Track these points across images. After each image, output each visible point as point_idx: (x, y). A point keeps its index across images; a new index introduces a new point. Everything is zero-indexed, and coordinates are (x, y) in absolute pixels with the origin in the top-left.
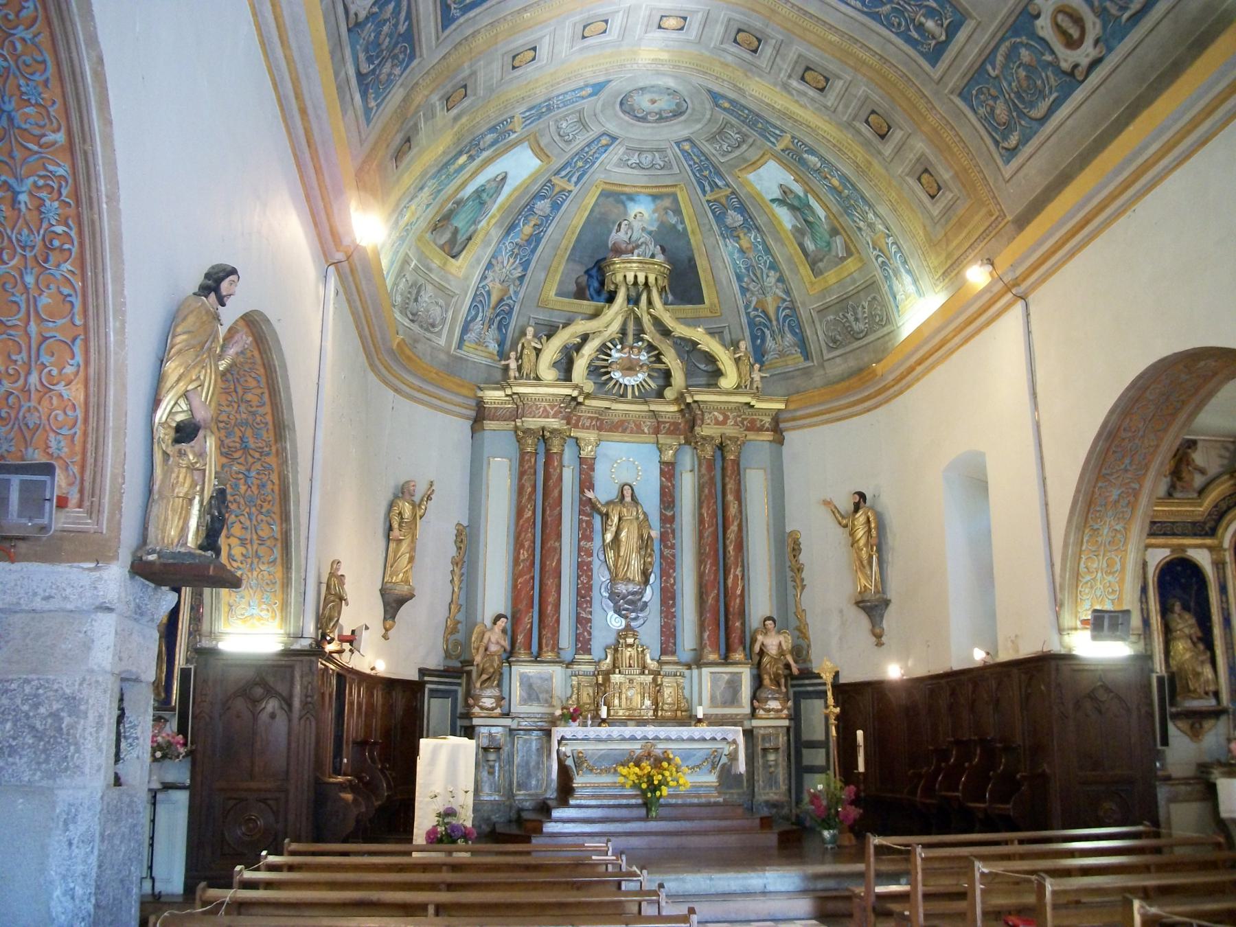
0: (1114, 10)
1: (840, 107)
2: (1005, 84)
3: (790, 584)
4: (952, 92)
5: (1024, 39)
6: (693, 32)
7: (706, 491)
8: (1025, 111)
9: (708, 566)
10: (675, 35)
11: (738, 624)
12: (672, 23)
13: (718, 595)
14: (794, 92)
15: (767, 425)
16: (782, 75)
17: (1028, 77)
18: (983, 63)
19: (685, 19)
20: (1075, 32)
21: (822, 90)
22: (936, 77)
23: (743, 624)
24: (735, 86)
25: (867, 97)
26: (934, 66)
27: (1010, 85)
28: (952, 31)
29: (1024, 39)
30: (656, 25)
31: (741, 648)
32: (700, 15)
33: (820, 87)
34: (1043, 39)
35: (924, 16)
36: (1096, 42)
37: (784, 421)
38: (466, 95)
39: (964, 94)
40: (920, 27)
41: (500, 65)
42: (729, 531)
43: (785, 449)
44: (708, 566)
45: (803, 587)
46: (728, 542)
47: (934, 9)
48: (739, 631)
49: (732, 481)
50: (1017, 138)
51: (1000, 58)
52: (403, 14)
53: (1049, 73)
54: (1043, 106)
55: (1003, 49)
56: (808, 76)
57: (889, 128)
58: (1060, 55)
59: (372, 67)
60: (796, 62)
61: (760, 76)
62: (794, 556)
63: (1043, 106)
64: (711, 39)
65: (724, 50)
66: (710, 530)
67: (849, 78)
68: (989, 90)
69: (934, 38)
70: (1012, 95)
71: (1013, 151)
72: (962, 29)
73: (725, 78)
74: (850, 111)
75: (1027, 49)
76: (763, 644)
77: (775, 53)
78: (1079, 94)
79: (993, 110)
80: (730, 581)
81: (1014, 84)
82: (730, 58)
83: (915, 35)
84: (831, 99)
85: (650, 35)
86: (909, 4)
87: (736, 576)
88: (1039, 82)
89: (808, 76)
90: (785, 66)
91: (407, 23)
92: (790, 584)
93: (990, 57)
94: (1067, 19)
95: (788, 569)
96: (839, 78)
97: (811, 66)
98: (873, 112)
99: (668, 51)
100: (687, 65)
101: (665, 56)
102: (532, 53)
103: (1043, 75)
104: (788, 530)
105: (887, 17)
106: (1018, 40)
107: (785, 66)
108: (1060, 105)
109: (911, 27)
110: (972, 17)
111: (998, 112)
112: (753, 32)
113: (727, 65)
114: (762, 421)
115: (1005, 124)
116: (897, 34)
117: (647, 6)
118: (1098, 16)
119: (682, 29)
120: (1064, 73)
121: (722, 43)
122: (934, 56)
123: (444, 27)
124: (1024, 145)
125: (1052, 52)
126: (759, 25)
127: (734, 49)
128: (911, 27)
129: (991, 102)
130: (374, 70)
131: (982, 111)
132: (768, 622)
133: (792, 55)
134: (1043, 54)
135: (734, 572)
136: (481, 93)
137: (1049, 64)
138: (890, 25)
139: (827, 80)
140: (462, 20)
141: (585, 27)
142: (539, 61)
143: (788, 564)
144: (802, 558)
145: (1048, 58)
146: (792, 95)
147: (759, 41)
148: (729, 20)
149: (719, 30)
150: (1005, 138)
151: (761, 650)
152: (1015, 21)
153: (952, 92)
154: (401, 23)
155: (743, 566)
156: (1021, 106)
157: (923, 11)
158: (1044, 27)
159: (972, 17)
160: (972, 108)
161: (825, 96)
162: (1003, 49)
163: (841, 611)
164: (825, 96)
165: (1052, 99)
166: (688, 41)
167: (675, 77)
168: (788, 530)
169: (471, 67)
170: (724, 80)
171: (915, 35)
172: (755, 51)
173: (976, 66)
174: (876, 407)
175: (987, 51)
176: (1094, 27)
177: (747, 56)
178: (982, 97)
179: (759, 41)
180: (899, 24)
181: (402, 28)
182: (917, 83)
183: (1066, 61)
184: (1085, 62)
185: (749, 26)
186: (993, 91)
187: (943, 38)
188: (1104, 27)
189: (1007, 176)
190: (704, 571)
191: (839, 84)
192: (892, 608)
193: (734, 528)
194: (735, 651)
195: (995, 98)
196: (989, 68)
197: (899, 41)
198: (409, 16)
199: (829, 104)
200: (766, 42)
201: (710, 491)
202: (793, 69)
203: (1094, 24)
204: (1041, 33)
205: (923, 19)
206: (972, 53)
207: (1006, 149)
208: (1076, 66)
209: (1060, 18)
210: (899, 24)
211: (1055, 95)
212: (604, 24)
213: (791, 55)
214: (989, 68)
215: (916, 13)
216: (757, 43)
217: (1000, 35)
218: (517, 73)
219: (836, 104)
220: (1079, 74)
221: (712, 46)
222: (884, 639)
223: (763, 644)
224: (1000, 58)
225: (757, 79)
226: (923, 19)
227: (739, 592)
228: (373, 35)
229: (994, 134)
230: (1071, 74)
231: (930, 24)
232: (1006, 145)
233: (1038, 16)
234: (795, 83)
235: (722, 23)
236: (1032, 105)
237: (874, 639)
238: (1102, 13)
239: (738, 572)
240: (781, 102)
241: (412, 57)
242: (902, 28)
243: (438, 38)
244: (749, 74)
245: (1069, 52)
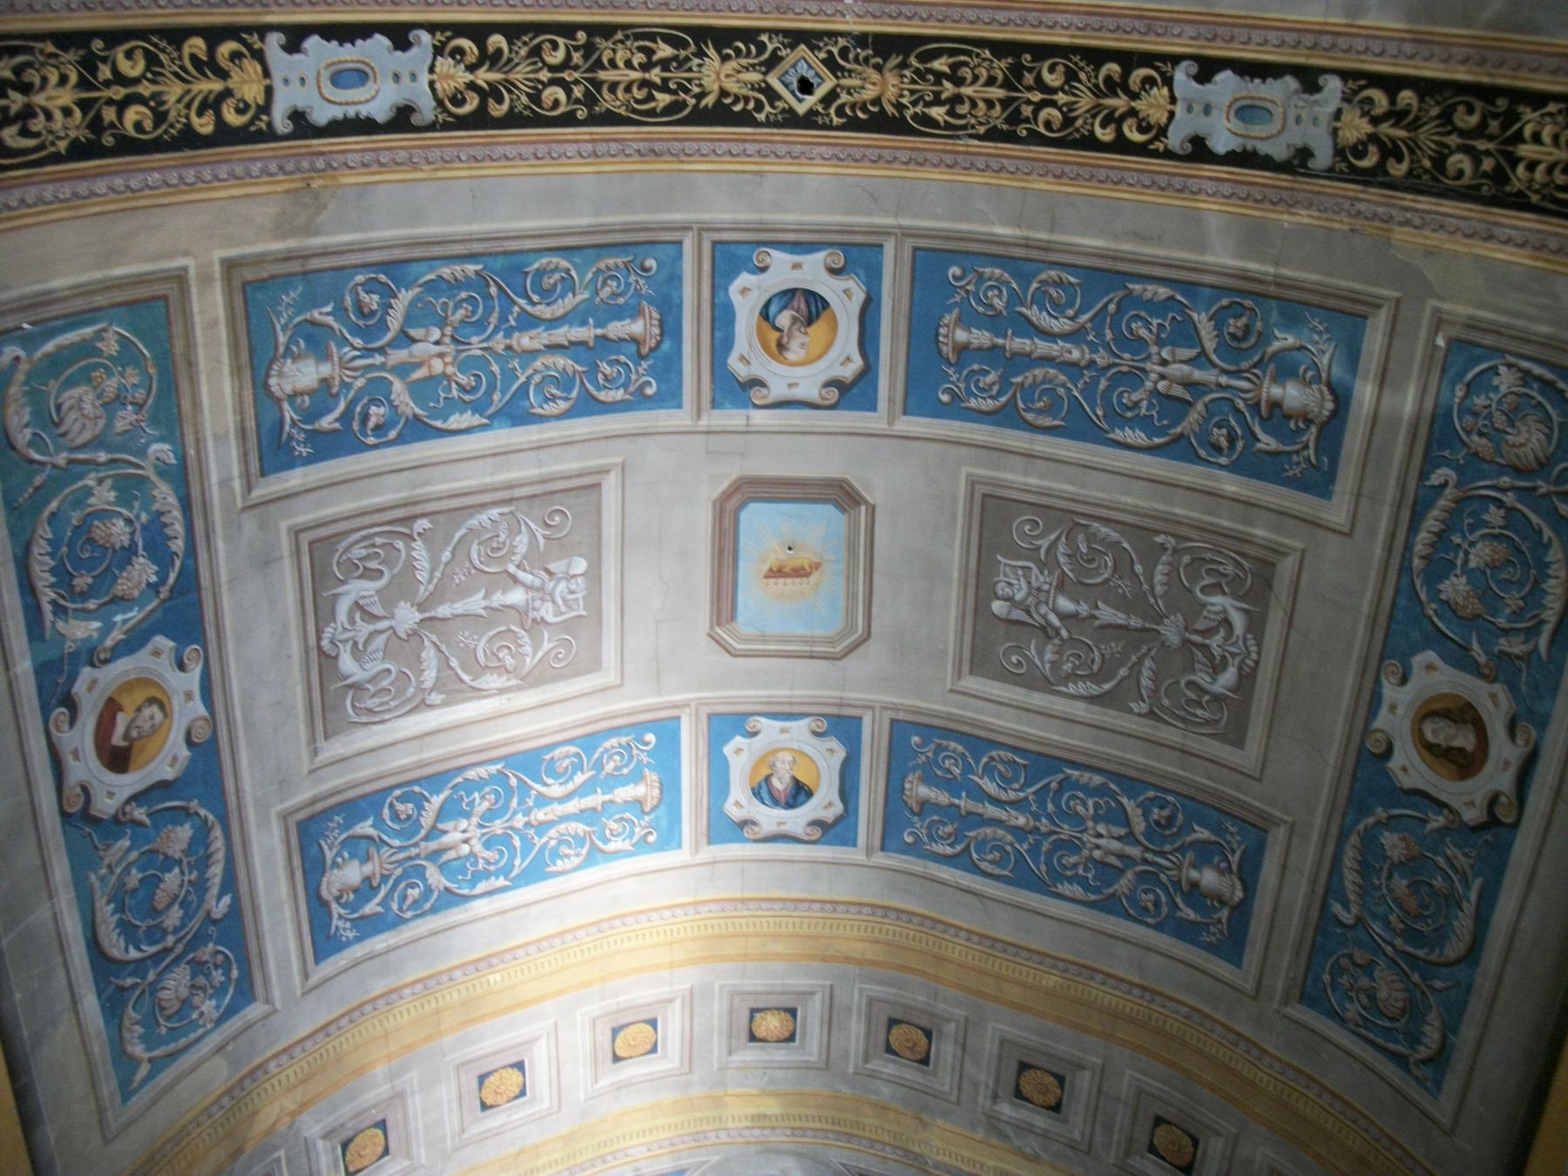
0: (1517, 647)
1: (1098, 1138)
2: (1377, 927)
4: (1286, 1001)
5: (1381, 813)
6: (812, 1045)
8: (1433, 957)
10: (780, 1054)
12: (771, 1024)
14: (1009, 1131)
16: (981, 1099)
17: (1414, 886)
18: (1324, 906)
19: (792, 1012)
20: (1464, 740)
21: (1056, 1108)
22: (1249, 986)
24: (906, 1151)
25: (1140, 1093)
26: (1238, 964)
27: (1387, 924)
28: (1248, 874)
29: (1381, 813)
30: (744, 1034)
32: (818, 998)
33: (1052, 1101)
34: (1416, 792)
35: (1194, 866)
36: (1512, 728)
38: (386, 1152)
39: (1310, 996)
40: (1194, 892)
41: (454, 1095)
47: (1209, 842)
50: (1437, 1023)
51: (1350, 877)
52: (216, 871)
53: (1451, 851)
54: (1463, 923)
55: (1350, 854)
56: (1029, 1082)
57: (1195, 1142)
58: (1455, 803)
59: (134, 954)
60: (1000, 1059)
61: (945, 1114)
63: (1463, 923)
64: (846, 1054)
65: (873, 1075)
67: (1099, 1062)
68: (1350, 956)
69: (1223, 903)
70: (1398, 942)
71: (1440, 1059)
72: (1268, 854)
73: (886, 1138)
74: (1116, 1137)
75: (1392, 831)
77: (959, 1052)
78: (1522, 849)
79: (1372, 997)
81: (1392, 918)
82: (886, 1090)
83: (1189, 914)
84: (1076, 1123)
85: (738, 1057)
86: (1162, 854)
88: (1438, 882)
89: (1029, 1082)
90: (982, 1077)
91: (227, 900)
93: (1332, 889)
94: (1441, 723)
96: (1081, 1067)
97: (1029, 1060)
98: (1159, 1121)
99: (777, 1095)
100: (817, 1125)
101: (772, 1107)
102: (515, 1076)
103: (1440, 860)
105: (1132, 898)
106: (1371, 820)
107: (982, 1077)
108: (1491, 908)
109: (1179, 900)
110: (1277, 823)
111: (1382, 994)
112: (916, 1020)
113: (882, 1108)
115: (1403, 1010)
116: (1158, 927)
117: (722, 987)
118: (1493, 680)
119: (791, 1038)
120: (1478, 829)
121: (866, 1060)
122: (1232, 946)
123: (320, 956)
124: (1455, 1032)
125: (1441, 805)
126: (921, 999)
127: (889, 1068)
128: (1179, 900)
129: (1364, 982)
130: (139, 967)
131: (1352, 1010)
133: (990, 1047)
134: (1425, 821)
136: (422, 1154)
137: (1442, 832)
138: (1138, 916)
139: (1061, 1080)
140: (358, 951)
141: (615, 1032)
142: (534, 1099)
145: (1438, 821)
146: (1006, 1137)
147: (928, 1034)
148: (871, 1001)
149: (855, 1030)
150: (1414, 1039)
152: (1352, 789)
153: (1286, 1001)
154: (215, 891)
156: (1420, 953)
157: (1190, 856)
158: (1409, 767)
159: (1277, 823)
160: (1333, 1014)
161: (1065, 1121)
162: (1350, 854)
164: (1065, 1121)
165: (1473, 896)
166: (807, 1067)
167: (798, 1155)
169: (391, 1077)
170: (884, 1144)
171: (1189, 914)
172: (925, 1061)
173: (1314, 914)
175: (1324, 875)
176: (1494, 704)
177: (912, 1074)
178: (1344, 980)
179: (928, 1034)
180: (1157, 904)
181: (220, 907)
182: (1219, 1017)
183: (1471, 804)
184: (1504, 781)
185: (905, 1006)
186: (1360, 956)
187: (1239, 894)
188: (1513, 688)
189: (1446, 1121)
191: (1083, 1083)
195: (1368, 968)
196: (1337, 908)
197: (1163, 941)
198: (230, 882)
199: (1077, 1136)
200: (940, 1032)
202: (997, 1080)
203: (1493, 697)
204: (1407, 782)
205: (1194, 874)
206: (1299, 891)
207: (1426, 1062)
208: (1493, 800)
209: (1428, 729)
210: (1157, 904)
211: (1476, 884)
212: (649, 1028)
213: (987, 1046)
214: (1337, 908)
215: (1179, 867)
216: (925, 1040)
217: (1334, 831)
218: (494, 1120)
219: (1088, 1130)
220: (1505, 815)
221: (851, 1070)
224: (1350, 877)
225: (940, 1122)
226: (1194, 874)
228: (135, 875)
229: (1391, 1046)
230: (1492, 821)
231: (1209, 878)
232: (1423, 1052)
233: (1388, 752)
234: (1006, 1109)
235: (859, 1012)
236: (1441, 936)
238: (1501, 669)
240: (992, 1163)
241: (246, 992)
242: (1165, 910)
243: (306, 975)
244: (925, 1117)
245: (1469, 784)
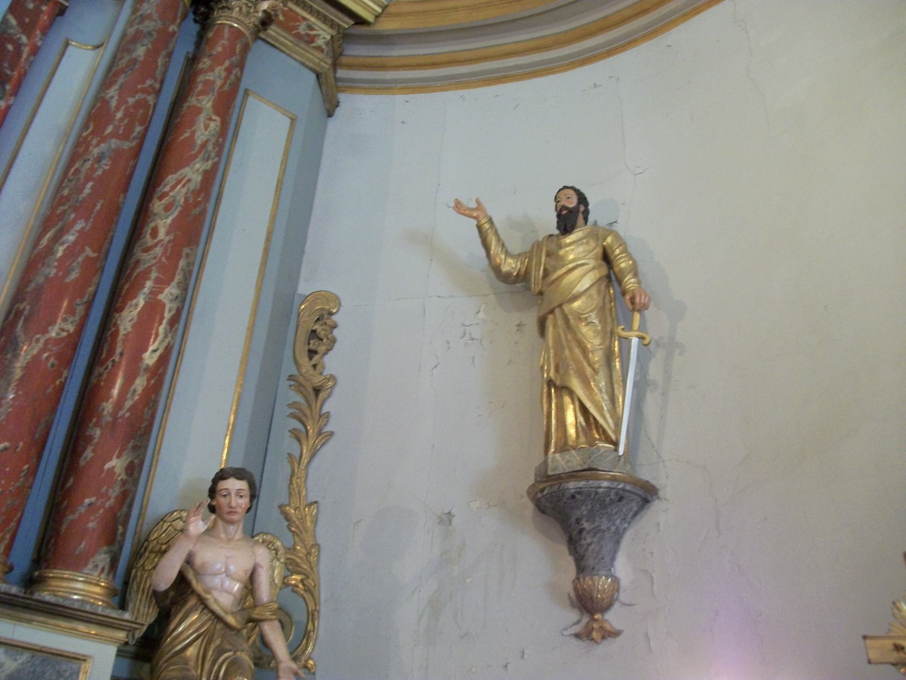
3: (284, 423)
7: (140, 51)
9: (71, 238)
11: (117, 464)
13: (74, 342)
15: (320, 42)
23: (133, 470)
31: (102, 559)
37: (350, 67)
42: (171, 179)
43: (333, 125)
44: (71, 238)
45: (325, 437)
46: (157, 206)
48: (115, 492)
49: (220, 71)
62: (312, 353)
66: (114, 143)
76: (189, 561)
80: (127, 320)
87: (153, 308)
92: (284, 423)
95: (284, 383)
104: (304, 288)
114: (310, 28)
132: (233, 484)
135: (154, 293)
143: (289, 368)
144: (332, 363)
151: (182, 582)
155: (184, 287)
163: (447, 518)
168: (304, 288)
174: (611, 51)
190: (50, 250)
192: (656, 512)
193: (193, 173)
194: (78, 564)
201: (152, 54)
222: (613, 618)
223: (189, 561)
227: (150, 358)
237: (573, 615)
239: (169, 294)
